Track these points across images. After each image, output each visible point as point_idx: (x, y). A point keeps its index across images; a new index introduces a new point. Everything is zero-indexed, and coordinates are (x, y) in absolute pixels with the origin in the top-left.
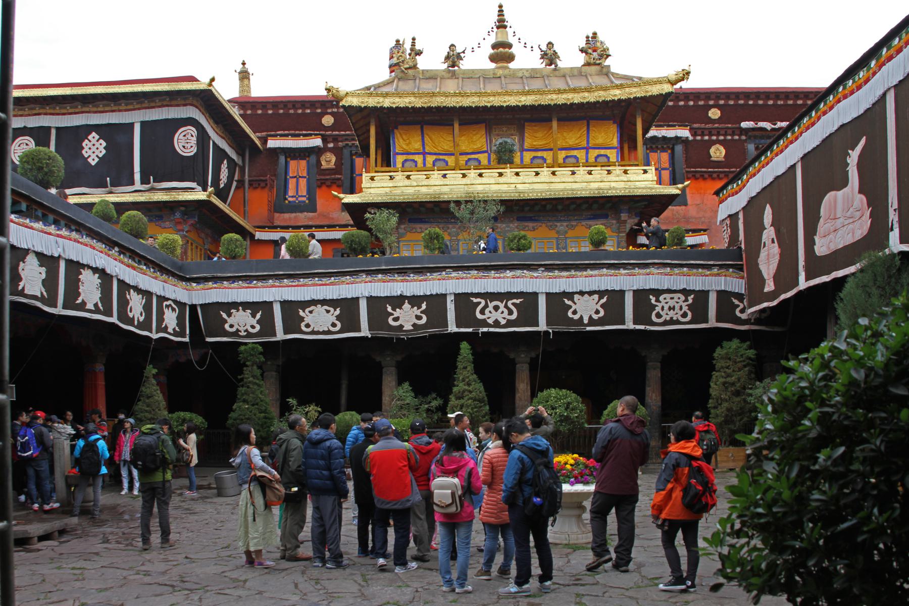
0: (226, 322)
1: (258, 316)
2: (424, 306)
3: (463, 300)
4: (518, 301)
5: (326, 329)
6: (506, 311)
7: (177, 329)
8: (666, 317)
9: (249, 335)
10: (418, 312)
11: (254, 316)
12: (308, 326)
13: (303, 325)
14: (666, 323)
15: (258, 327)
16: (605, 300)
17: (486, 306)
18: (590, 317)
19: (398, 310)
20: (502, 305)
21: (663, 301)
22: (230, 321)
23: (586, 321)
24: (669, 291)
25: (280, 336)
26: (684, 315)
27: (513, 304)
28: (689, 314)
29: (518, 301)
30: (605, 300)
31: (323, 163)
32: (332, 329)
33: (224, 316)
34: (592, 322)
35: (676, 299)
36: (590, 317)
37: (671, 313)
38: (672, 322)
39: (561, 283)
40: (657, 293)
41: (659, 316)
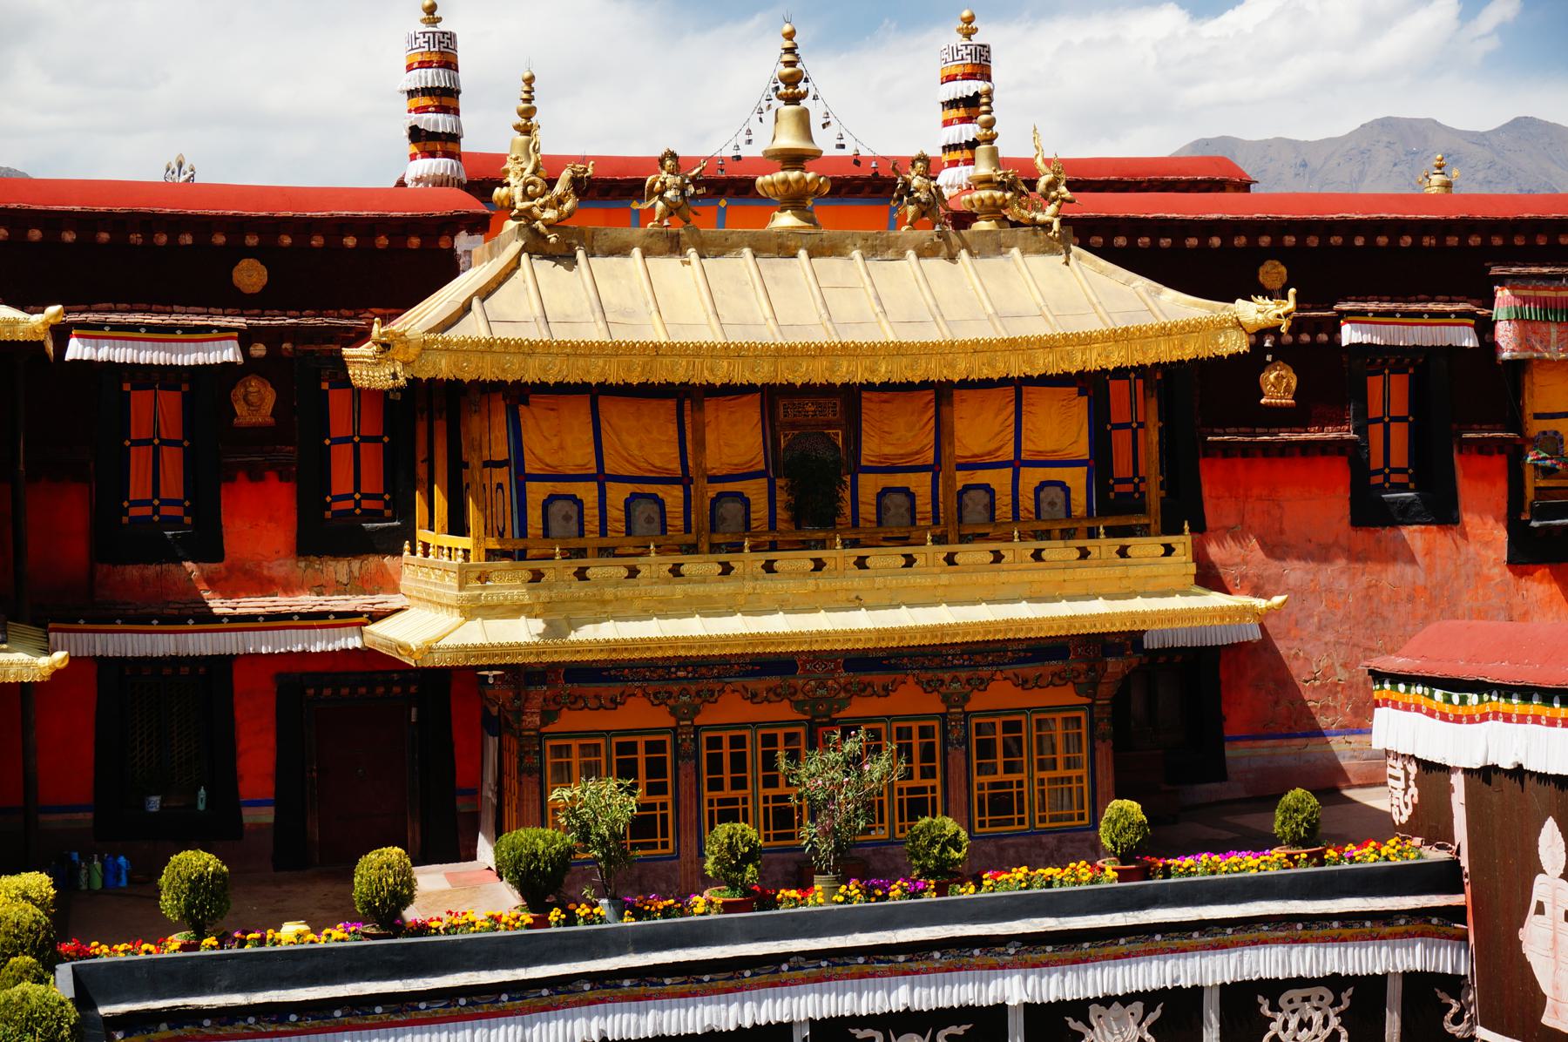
24: (1300, 982)
30: (1158, 1012)
31: (240, 408)
40: (1274, 988)
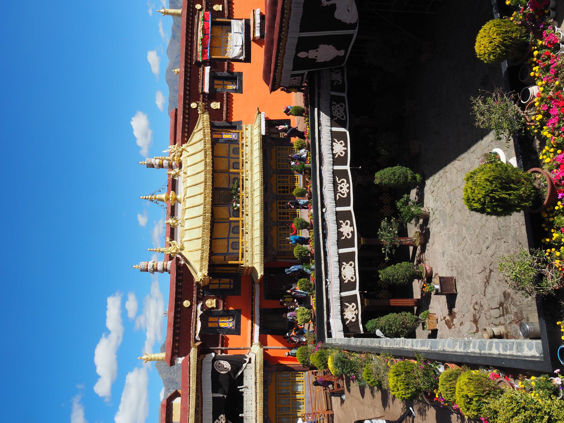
1: (347, 304)
2: (341, 221)
4: (337, 179)
6: (343, 184)
10: (344, 224)
11: (347, 307)
12: (352, 278)
15: (353, 304)
16: (336, 140)
17: (340, 193)
23: (346, 149)
26: (342, 106)
29: (337, 179)
30: (336, 140)
32: (353, 266)
33: (348, 322)
37: (341, 111)
38: (345, 111)
39: (327, 159)
41: (343, 117)
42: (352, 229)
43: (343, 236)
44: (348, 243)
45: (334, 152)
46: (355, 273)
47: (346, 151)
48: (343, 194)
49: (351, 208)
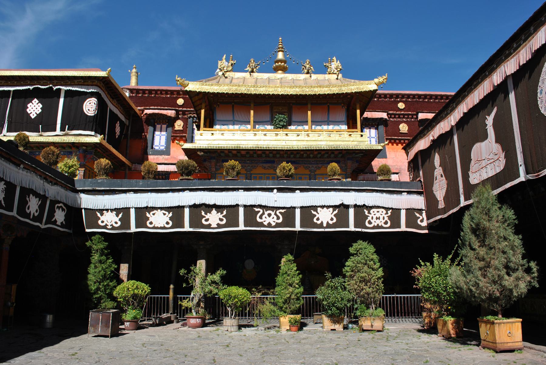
0: (99, 219)
1: (120, 216)
2: (225, 213)
3: (249, 209)
4: (283, 211)
5: (163, 226)
7: (64, 223)
8: (374, 224)
9: (113, 228)
11: (117, 216)
12: (151, 223)
13: (148, 222)
14: (374, 228)
15: (119, 223)
17: (263, 214)
18: (328, 222)
19: (208, 214)
20: (273, 213)
21: (373, 214)
22: (102, 218)
23: (325, 225)
25: (133, 229)
26: (386, 223)
27: (280, 213)
28: (389, 222)
33: (99, 215)
34: (329, 226)
35: (380, 213)
36: (328, 222)
37: (378, 222)
38: (378, 227)
41: (370, 223)
42: (214, 225)
43: (206, 214)
44: (196, 221)
45: (319, 209)
46: (157, 228)
47: (321, 226)
48: (261, 217)
49: (242, 227)
